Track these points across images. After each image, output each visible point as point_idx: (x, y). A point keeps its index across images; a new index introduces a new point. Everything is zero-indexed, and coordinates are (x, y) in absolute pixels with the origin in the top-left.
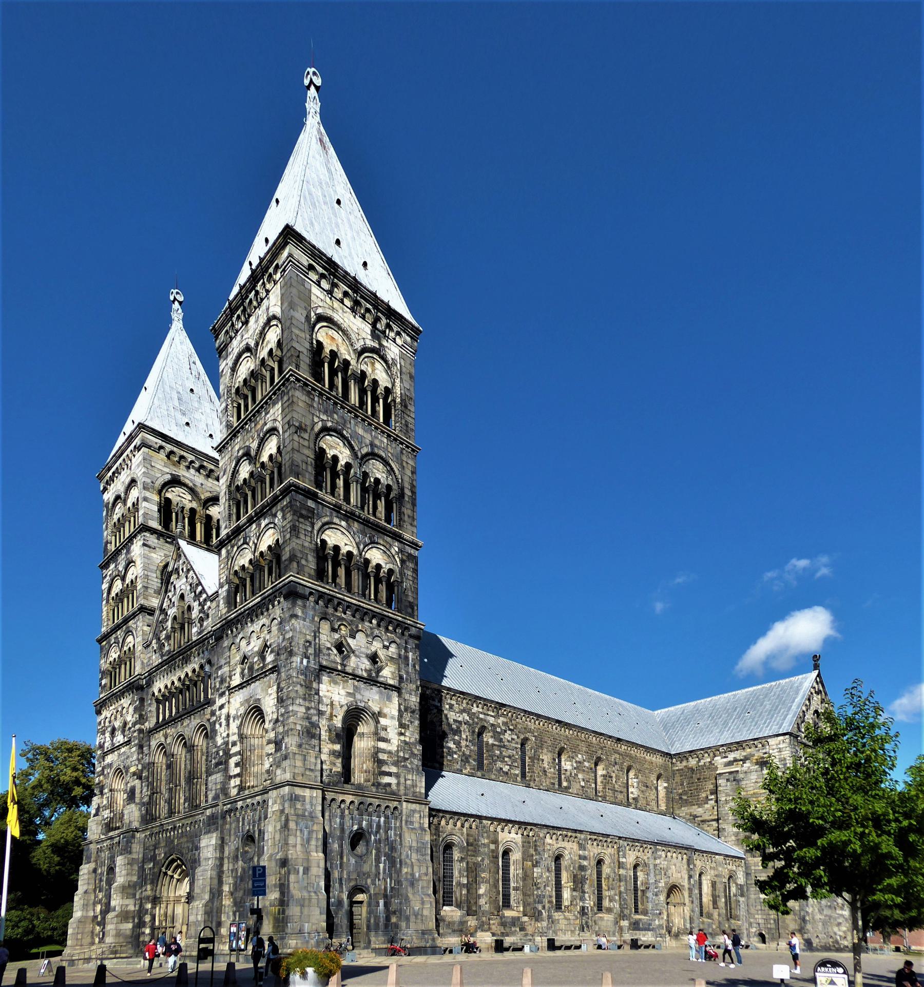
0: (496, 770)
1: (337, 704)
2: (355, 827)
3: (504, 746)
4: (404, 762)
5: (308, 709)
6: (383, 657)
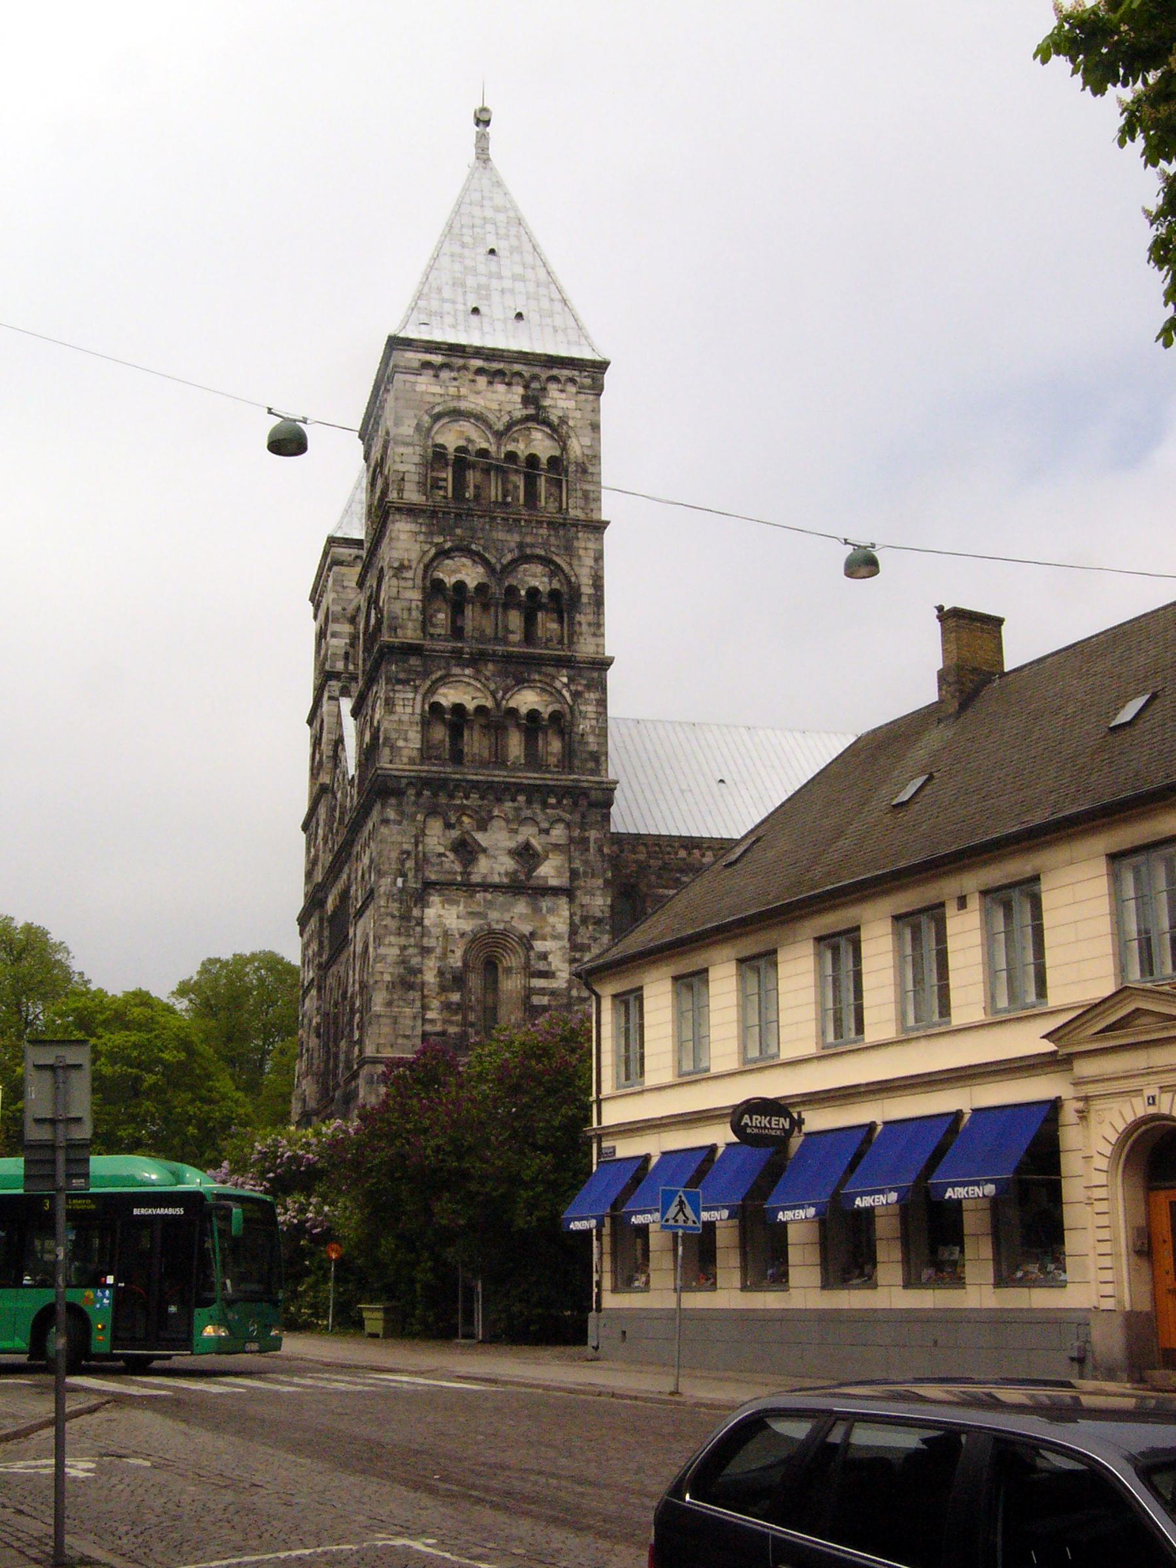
1: (456, 933)
4: (580, 1004)
5: (403, 948)
6: (539, 848)
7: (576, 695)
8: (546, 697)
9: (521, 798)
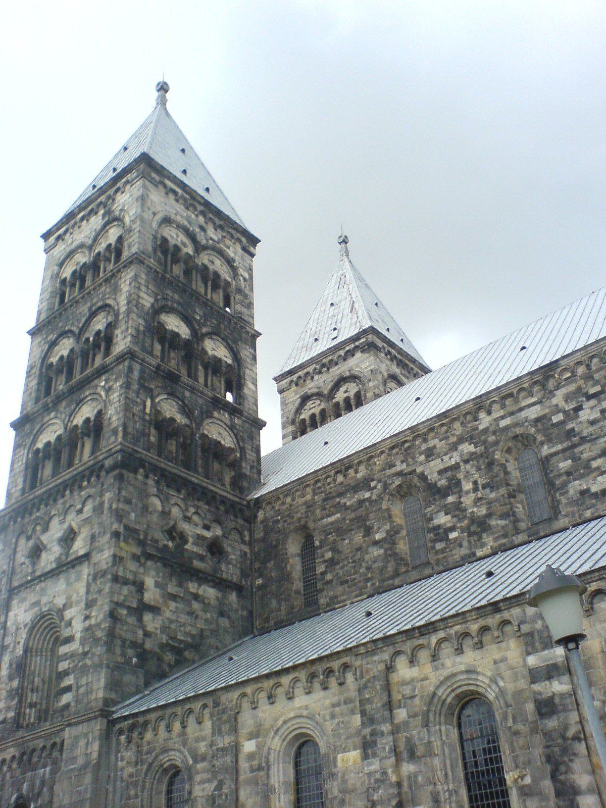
0: (571, 503)
3: (583, 440)
7: (108, 390)
9: (68, 492)
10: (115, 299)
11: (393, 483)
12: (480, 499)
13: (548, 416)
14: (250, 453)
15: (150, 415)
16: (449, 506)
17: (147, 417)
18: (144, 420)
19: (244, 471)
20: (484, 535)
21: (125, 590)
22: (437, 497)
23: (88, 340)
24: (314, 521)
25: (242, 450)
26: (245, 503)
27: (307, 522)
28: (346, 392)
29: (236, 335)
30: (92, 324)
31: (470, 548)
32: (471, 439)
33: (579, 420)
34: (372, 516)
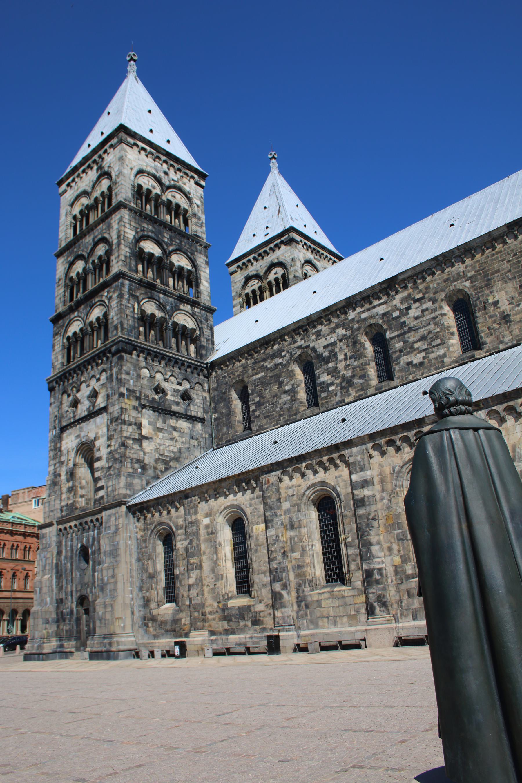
0: (402, 370)
2: (79, 545)
3: (411, 329)
7: (110, 299)
8: (102, 307)
10: (109, 234)
11: (296, 353)
12: (348, 365)
13: (391, 312)
14: (206, 330)
15: (137, 314)
16: (329, 370)
17: (136, 316)
18: (134, 318)
19: (202, 343)
20: (350, 389)
21: (130, 429)
22: (323, 363)
23: (93, 261)
24: (248, 377)
25: (201, 329)
26: (204, 365)
27: (243, 378)
28: (275, 274)
29: (194, 249)
30: (96, 250)
31: (342, 397)
32: (344, 325)
33: (408, 316)
34: (283, 374)
